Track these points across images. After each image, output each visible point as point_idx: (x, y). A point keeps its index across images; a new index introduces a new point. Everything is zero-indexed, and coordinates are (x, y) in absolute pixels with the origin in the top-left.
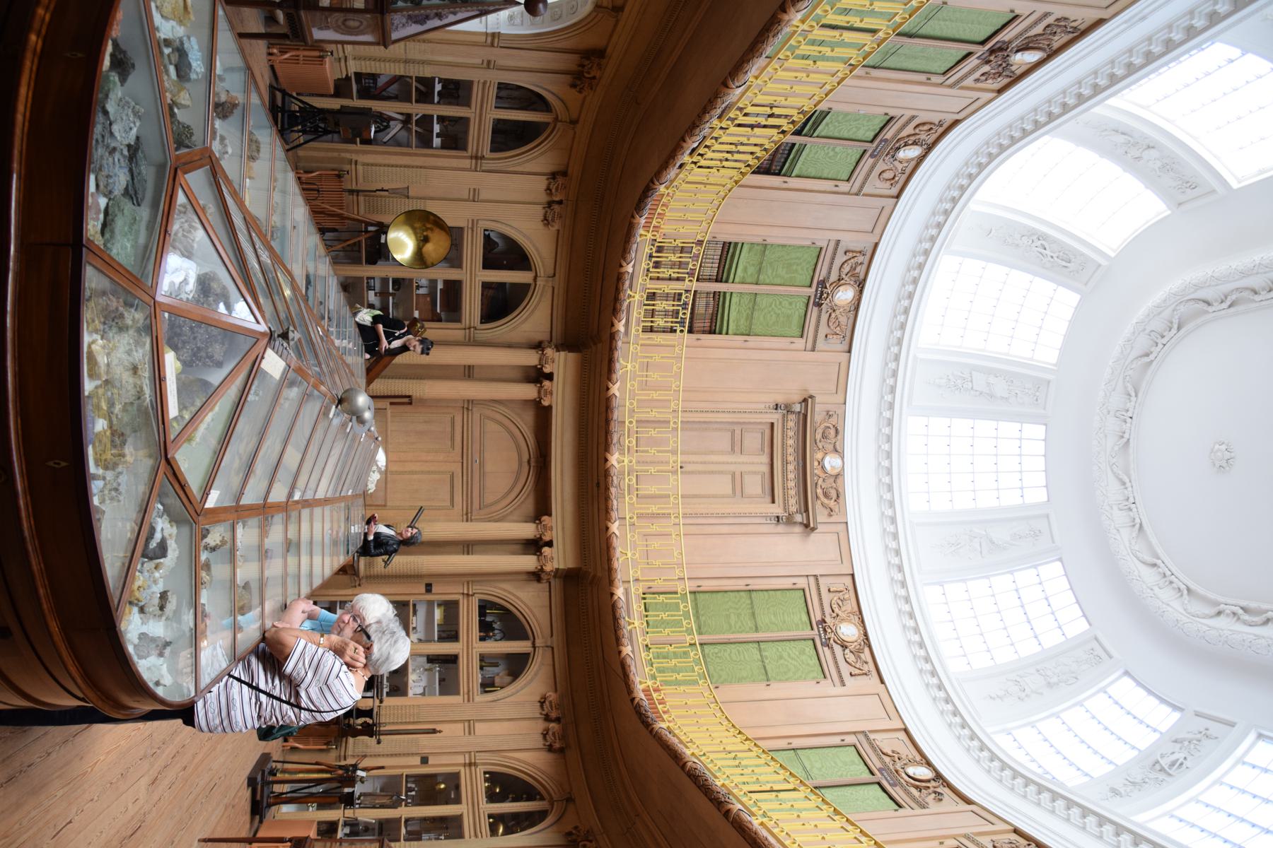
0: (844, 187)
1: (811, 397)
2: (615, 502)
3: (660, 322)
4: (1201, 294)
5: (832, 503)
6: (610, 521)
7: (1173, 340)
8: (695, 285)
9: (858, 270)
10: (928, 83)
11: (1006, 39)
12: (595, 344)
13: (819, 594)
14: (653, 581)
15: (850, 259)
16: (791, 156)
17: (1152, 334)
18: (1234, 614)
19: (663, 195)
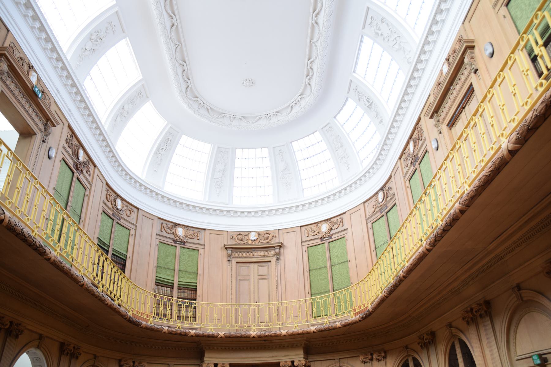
0: (133, 232)
1: (225, 246)
2: (273, 332)
3: (191, 314)
5: (271, 236)
6: (281, 335)
7: (202, 100)
8: (175, 298)
9: (169, 226)
10: (89, 196)
11: (72, 163)
12: (201, 344)
13: (309, 240)
14: (307, 313)
15: (165, 229)
16: (118, 255)
17: (199, 108)
19: (132, 313)
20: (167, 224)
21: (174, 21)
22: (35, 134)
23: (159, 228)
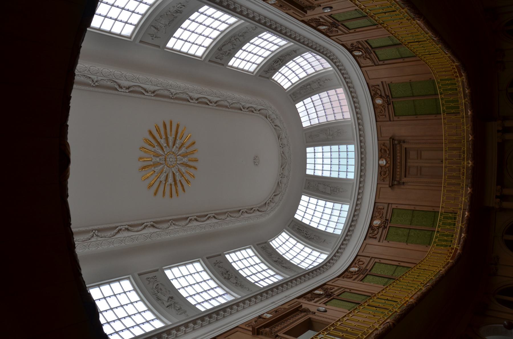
1: (390, 187)
2: (471, 147)
4: (261, 213)
7: (268, 199)
9: (372, 231)
10: (350, 289)
11: (326, 298)
18: (255, 110)
20: (370, 234)
21: (212, 215)
22: (310, 318)
23: (374, 240)
